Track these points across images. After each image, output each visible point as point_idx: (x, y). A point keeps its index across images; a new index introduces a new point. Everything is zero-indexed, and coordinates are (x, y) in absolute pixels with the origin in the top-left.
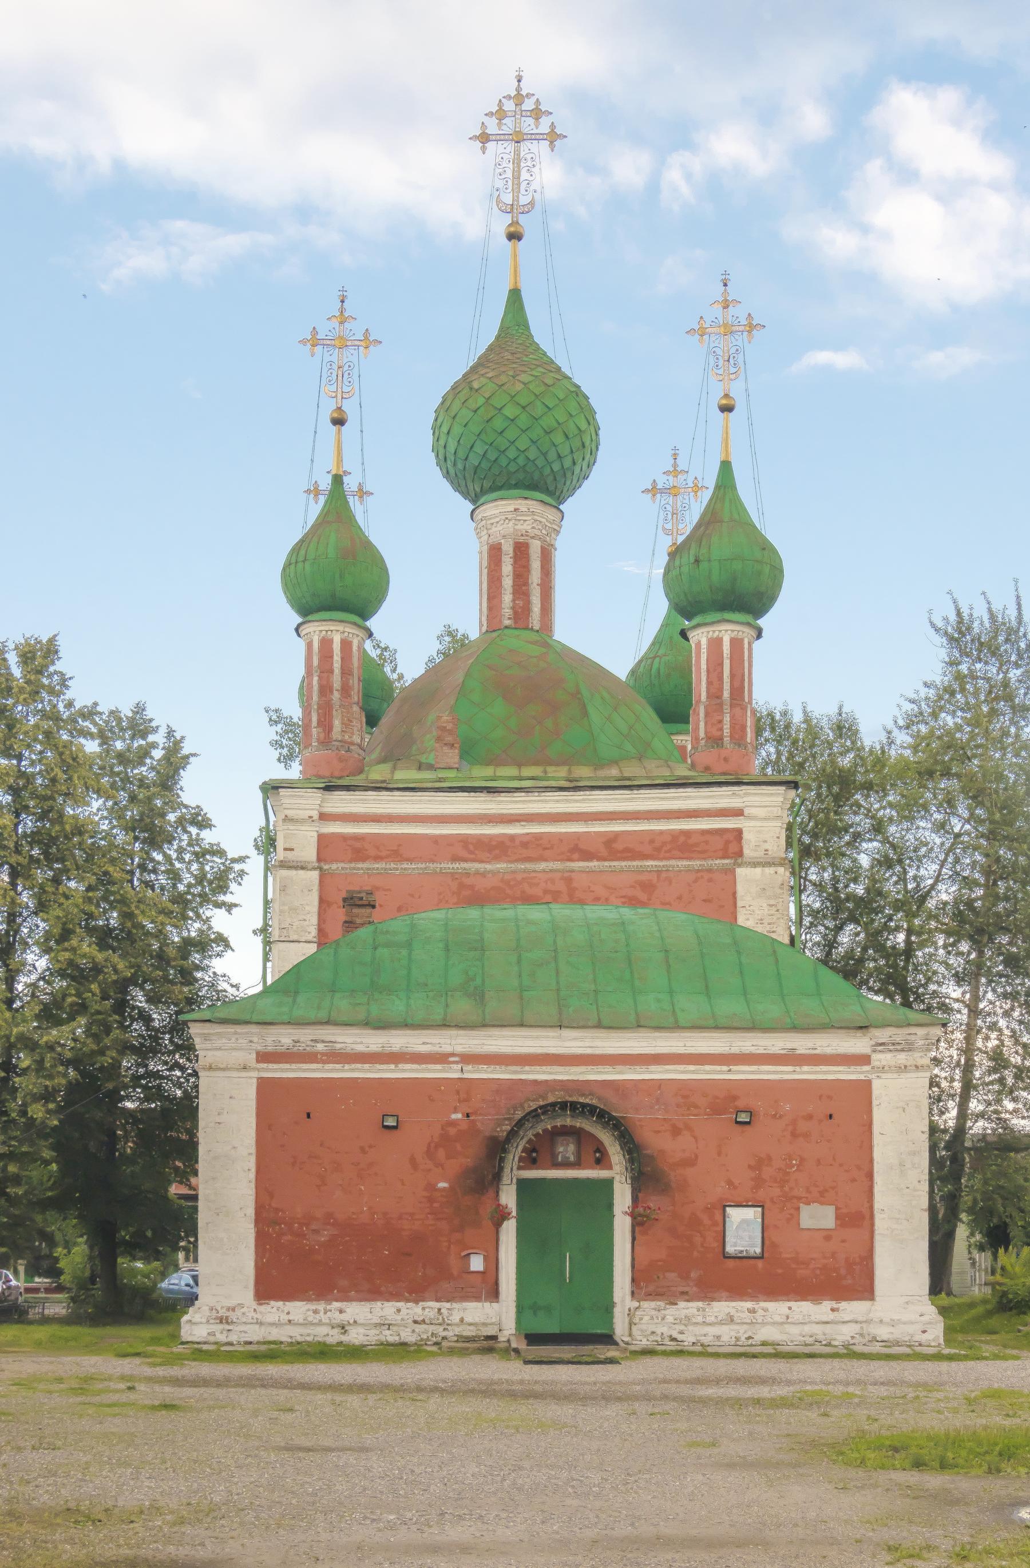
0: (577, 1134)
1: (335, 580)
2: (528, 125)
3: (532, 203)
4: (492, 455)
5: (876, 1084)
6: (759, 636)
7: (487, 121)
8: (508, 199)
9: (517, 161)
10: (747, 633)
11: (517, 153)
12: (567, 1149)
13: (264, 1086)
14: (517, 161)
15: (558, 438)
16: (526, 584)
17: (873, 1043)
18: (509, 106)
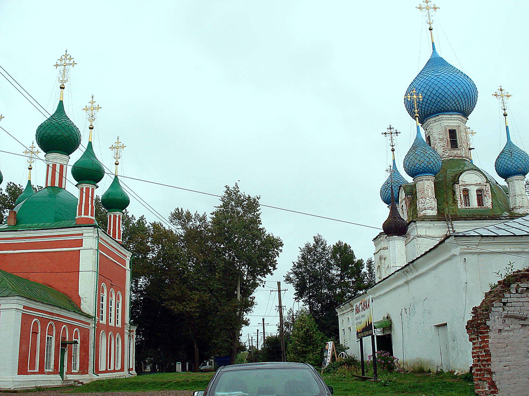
7: (58, 61)
8: (61, 79)
9: (65, 69)
14: (64, 71)
18: (63, 57)
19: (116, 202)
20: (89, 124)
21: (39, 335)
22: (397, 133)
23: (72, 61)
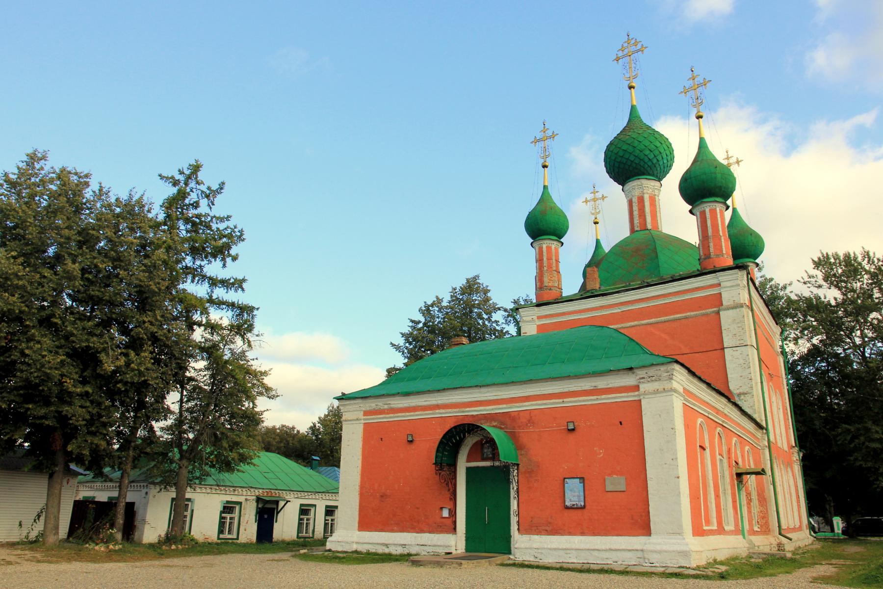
4: (622, 166)
5: (644, 403)
13: (368, 428)
15: (647, 152)
17: (638, 377)
19: (745, 250)
21: (708, 450)
23: (639, 47)
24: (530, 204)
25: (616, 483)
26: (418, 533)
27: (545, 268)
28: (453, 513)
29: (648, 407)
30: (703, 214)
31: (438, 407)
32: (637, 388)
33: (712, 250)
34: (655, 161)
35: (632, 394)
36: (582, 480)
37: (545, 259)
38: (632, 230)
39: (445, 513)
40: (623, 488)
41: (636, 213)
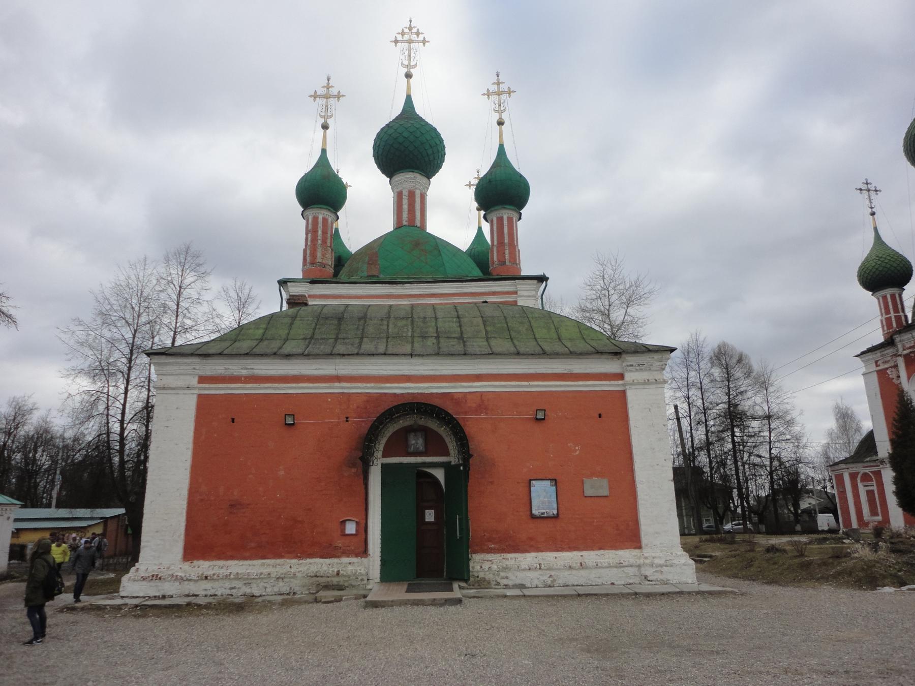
0: (426, 432)
1: (321, 192)
2: (414, 37)
3: (416, 65)
5: (630, 394)
6: (520, 219)
9: (410, 50)
10: (515, 216)
11: (410, 47)
12: (417, 442)
13: (204, 403)
14: (410, 50)
15: (427, 147)
16: (414, 207)
18: (406, 30)
20: (496, 117)
22: (876, 191)
23: (421, 38)
24: (305, 165)
25: (597, 487)
26: (299, 558)
27: (320, 242)
28: (363, 529)
29: (636, 401)
30: (500, 220)
31: (338, 379)
32: (621, 376)
33: (507, 257)
34: (431, 158)
35: (616, 382)
36: (555, 482)
37: (320, 232)
38: (399, 226)
39: (351, 528)
40: (605, 492)
41: (405, 206)
